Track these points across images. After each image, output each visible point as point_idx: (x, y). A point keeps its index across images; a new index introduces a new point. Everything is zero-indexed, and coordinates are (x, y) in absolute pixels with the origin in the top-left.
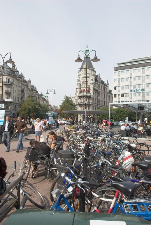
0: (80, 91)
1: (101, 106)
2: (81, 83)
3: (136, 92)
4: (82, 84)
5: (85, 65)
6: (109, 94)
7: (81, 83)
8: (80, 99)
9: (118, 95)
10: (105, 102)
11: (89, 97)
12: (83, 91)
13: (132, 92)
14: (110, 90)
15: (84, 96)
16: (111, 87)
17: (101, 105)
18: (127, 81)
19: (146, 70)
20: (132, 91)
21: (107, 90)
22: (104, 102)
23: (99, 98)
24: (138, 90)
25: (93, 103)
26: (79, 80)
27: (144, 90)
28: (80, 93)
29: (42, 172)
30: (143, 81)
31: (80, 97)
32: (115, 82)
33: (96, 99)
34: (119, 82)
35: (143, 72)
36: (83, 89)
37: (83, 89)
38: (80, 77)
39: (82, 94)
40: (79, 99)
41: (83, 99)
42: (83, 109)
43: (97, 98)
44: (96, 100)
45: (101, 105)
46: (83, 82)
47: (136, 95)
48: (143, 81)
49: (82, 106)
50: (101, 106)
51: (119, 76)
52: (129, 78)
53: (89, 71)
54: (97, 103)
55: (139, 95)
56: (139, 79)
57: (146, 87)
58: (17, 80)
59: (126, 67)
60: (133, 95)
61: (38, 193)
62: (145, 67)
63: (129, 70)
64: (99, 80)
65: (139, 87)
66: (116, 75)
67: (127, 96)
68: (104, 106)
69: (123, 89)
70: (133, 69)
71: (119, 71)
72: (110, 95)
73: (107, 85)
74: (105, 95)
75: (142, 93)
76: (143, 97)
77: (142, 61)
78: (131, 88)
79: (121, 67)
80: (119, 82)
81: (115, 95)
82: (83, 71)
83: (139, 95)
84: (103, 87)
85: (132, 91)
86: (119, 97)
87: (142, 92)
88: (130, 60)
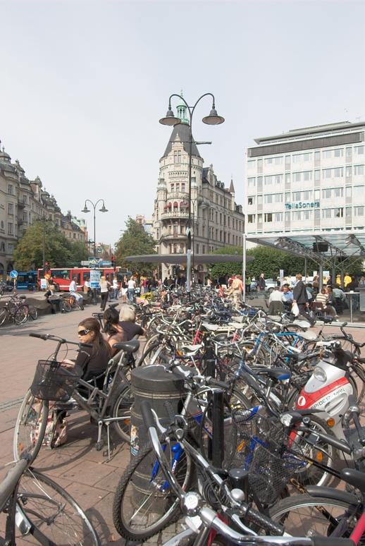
0: (165, 208)
1: (215, 243)
2: (169, 188)
3: (299, 209)
4: (169, 190)
6: (235, 215)
7: (169, 188)
8: (166, 227)
9: (256, 216)
10: (225, 233)
11: (186, 222)
12: (172, 207)
13: (292, 210)
14: (238, 204)
15: (174, 220)
16: (239, 198)
17: (216, 241)
18: (279, 182)
19: (324, 155)
20: (290, 207)
21: (230, 205)
22: (223, 234)
23: (211, 224)
24: (305, 206)
25: (198, 237)
26: (162, 180)
27: (318, 204)
28: (166, 211)
29: (80, 425)
30: (317, 182)
31: (166, 222)
32: (250, 186)
33: (204, 227)
34: (260, 184)
35: (317, 161)
36: (172, 202)
37: (172, 202)
38: (166, 171)
39: (170, 215)
41: (172, 227)
42: (173, 252)
43: (206, 224)
44: (203, 230)
45: (216, 241)
46: (173, 185)
47: (299, 218)
48: (317, 182)
49: (170, 245)
50: (215, 243)
51: (260, 169)
52: (284, 176)
54: (206, 236)
55: (307, 218)
56: (306, 178)
57: (323, 197)
58: (6, 178)
59: (276, 147)
60: (293, 217)
61: (75, 507)
62: (322, 149)
63: (284, 155)
64: (211, 179)
65: (307, 198)
66: (253, 168)
67: (278, 220)
68: (222, 244)
69: (270, 201)
70: (291, 154)
71: (260, 158)
72: (239, 217)
73: (231, 193)
74: (225, 216)
75: (313, 212)
76: (317, 221)
77: (314, 135)
78: (288, 201)
79: (265, 149)
80: (260, 184)
81: (250, 217)
82: (173, 157)
83: (307, 218)
84: (221, 198)
85: (290, 207)
86: (260, 222)
87: (313, 208)
88: (286, 132)
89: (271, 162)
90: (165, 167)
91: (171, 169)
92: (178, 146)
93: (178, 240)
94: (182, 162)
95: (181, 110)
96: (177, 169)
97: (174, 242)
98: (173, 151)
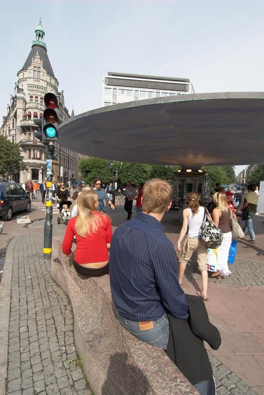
0: (25, 116)
4: (28, 99)
5: (36, 59)
7: (28, 99)
8: (25, 134)
12: (32, 116)
31: (25, 129)
36: (32, 111)
37: (32, 111)
40: (23, 134)
41: (32, 134)
42: (32, 156)
45: (66, 154)
46: (31, 97)
49: (30, 150)
51: (115, 96)
53: (46, 75)
63: (134, 89)
70: (139, 89)
71: (115, 87)
82: (32, 71)
89: (123, 93)
90: (25, 79)
91: (31, 82)
92: (37, 61)
93: (38, 146)
94: (41, 78)
95: (40, 35)
96: (37, 83)
97: (34, 148)
98: (32, 66)
